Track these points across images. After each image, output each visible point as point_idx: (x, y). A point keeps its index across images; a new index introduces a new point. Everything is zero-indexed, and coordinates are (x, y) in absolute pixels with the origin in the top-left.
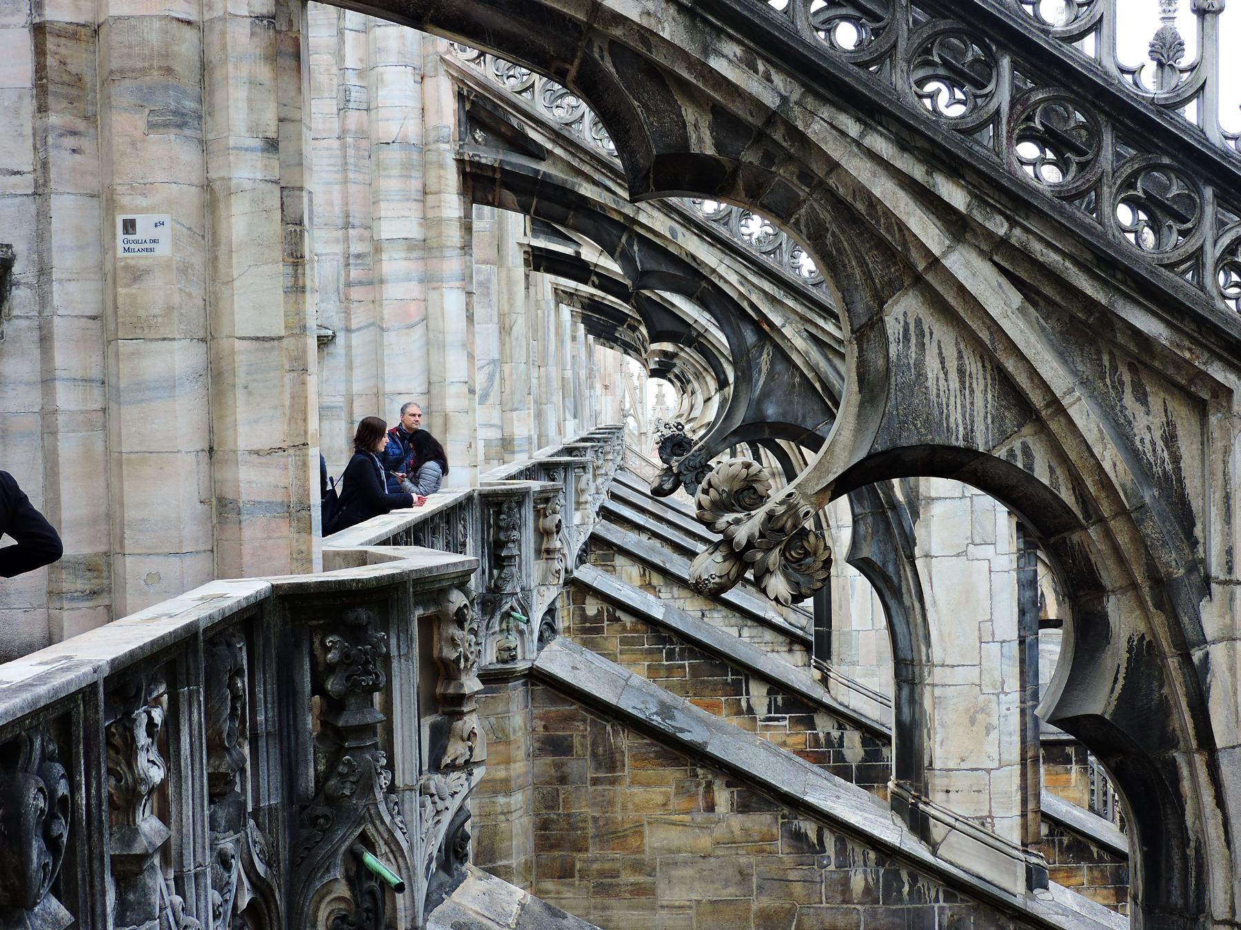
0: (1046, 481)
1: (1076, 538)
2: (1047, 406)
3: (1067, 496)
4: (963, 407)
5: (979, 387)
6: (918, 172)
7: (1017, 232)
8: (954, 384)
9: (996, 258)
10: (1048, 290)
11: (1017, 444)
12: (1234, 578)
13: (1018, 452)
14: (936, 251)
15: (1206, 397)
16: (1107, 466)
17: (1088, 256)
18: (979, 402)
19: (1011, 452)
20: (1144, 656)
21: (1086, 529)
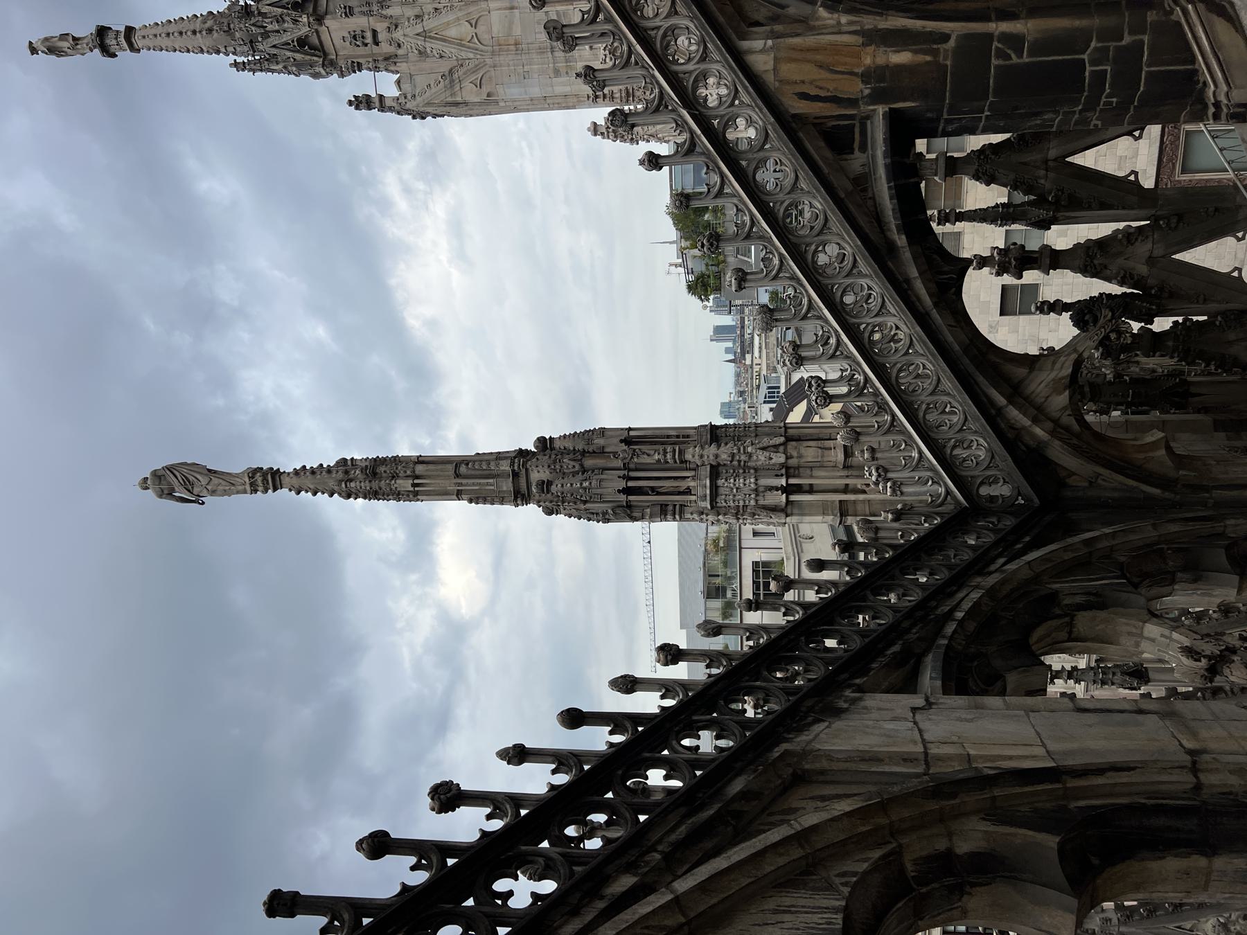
0: (865, 865)
1: (909, 867)
2: (803, 847)
3: (877, 854)
4: (806, 913)
5: (787, 901)
6: (601, 905)
7: (660, 848)
8: (787, 917)
9: (679, 873)
10: (708, 845)
11: (837, 881)
12: (922, 757)
13: (844, 880)
14: (670, 897)
15: (791, 770)
16: (848, 809)
17: (683, 810)
18: (802, 902)
19: (845, 884)
20: (995, 813)
21: (900, 846)
